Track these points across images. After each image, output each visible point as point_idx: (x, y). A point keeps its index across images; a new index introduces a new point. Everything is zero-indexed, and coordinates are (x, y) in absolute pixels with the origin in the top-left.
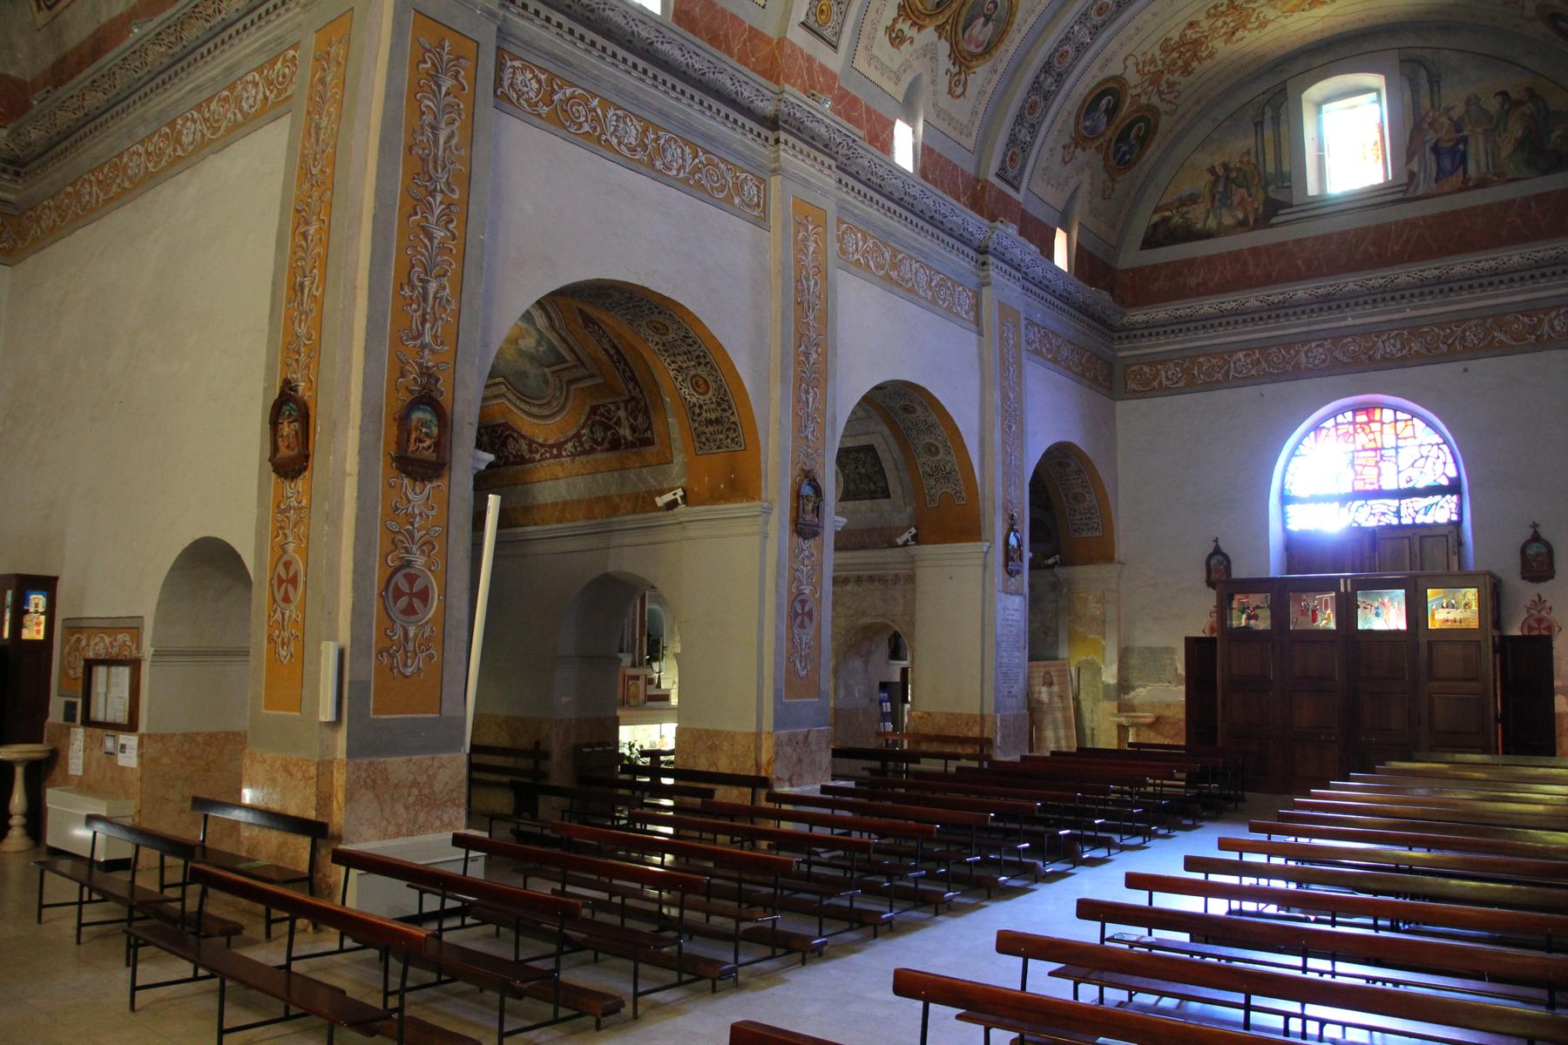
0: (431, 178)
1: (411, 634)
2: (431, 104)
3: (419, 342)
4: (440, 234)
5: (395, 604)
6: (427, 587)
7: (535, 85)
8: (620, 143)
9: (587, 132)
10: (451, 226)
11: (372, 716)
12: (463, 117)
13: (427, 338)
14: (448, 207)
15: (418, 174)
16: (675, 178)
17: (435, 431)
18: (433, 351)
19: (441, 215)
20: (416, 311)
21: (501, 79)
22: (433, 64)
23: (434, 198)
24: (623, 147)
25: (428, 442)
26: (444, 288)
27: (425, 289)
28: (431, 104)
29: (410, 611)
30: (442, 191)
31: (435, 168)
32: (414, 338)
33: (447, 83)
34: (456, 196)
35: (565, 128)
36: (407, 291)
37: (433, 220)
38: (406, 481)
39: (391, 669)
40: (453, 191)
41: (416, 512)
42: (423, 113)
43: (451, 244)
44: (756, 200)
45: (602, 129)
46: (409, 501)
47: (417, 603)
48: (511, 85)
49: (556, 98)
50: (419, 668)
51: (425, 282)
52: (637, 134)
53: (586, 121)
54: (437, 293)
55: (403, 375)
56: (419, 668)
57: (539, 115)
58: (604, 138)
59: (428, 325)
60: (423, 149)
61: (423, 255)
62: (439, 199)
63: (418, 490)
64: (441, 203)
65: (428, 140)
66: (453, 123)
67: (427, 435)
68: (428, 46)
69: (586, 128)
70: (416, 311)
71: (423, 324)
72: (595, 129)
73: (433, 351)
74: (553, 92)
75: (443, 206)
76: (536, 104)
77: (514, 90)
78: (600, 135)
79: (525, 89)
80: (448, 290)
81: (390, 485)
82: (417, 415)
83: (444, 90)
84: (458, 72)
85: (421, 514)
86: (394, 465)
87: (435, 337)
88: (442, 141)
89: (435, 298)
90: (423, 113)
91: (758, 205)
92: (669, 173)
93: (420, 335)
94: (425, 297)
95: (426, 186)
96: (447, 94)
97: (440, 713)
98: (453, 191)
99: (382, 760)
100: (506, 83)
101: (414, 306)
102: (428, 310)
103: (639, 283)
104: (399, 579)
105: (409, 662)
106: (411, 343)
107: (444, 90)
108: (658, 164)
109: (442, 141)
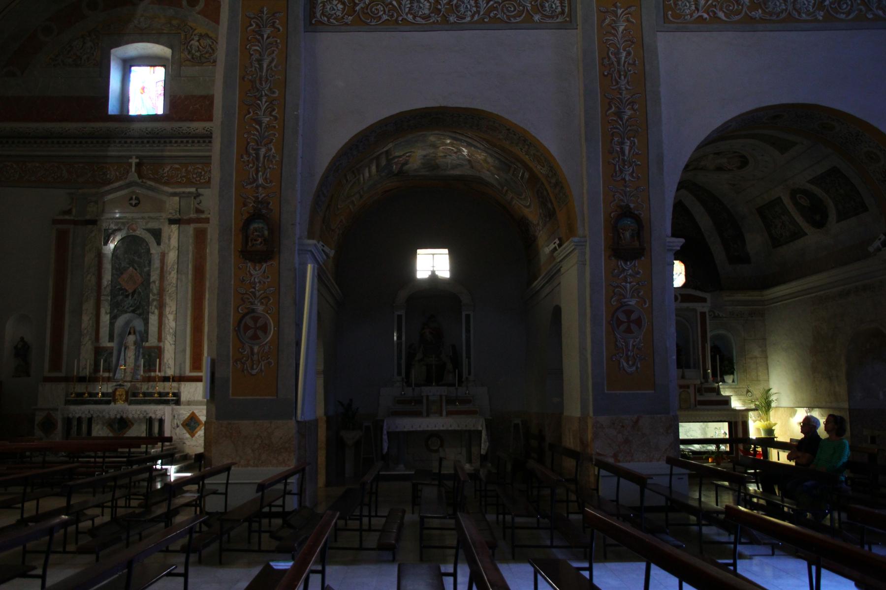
0: (258, 90)
1: (256, 350)
2: (258, 48)
3: (255, 185)
4: (266, 120)
5: (245, 333)
6: (266, 323)
7: (340, 6)
8: (414, 17)
9: (386, 20)
10: (274, 113)
11: (231, 397)
12: (280, 46)
13: (261, 181)
14: (271, 103)
15: (249, 90)
16: (470, 22)
17: (266, 233)
18: (264, 188)
19: (267, 108)
20: (252, 167)
21: (315, 13)
22: (257, 25)
23: (261, 101)
24: (418, 19)
25: (260, 240)
26: (271, 149)
27: (257, 155)
28: (258, 48)
29: (255, 337)
30: (266, 95)
31: (261, 84)
32: (251, 183)
33: (267, 32)
34: (276, 95)
35: (367, 24)
36: (245, 158)
37: (261, 113)
38: (249, 264)
39: (243, 371)
40: (274, 93)
41: (256, 280)
42: (252, 55)
43: (275, 124)
44: (559, 9)
45: (398, 13)
46: (251, 275)
47: (260, 333)
48: (323, 14)
49: (357, 8)
50: (261, 370)
51: (257, 151)
52: (430, 6)
53: (385, 13)
54: (266, 153)
55: (245, 205)
56: (261, 370)
57: (346, 24)
58: (400, 18)
59: (260, 174)
60: (252, 76)
61: (254, 135)
62: (264, 100)
63: (257, 268)
64: (266, 102)
65: (255, 69)
66: (273, 53)
67: (258, 236)
68: (252, 16)
69: (385, 17)
70: (252, 167)
71: (257, 174)
72: (392, 16)
73: (264, 188)
74: (356, 5)
75: (268, 103)
76: (343, 18)
77: (325, 16)
78: (397, 18)
79: (333, 12)
80: (273, 150)
81: (239, 268)
82: (255, 225)
83: (265, 36)
84: (274, 22)
85: (260, 282)
86: (241, 256)
87: (266, 179)
88: (265, 66)
89: (264, 157)
90: (252, 55)
91: (563, 13)
92: (464, 21)
93: (255, 180)
94: (257, 159)
95: (255, 96)
96: (268, 38)
97: (277, 396)
98: (274, 93)
99: (236, 422)
100: (318, 15)
101: (251, 165)
102: (260, 165)
103: (437, 105)
104: (248, 320)
105: (255, 367)
106: (249, 187)
107: (265, 36)
108: (452, 19)
109: (265, 66)
